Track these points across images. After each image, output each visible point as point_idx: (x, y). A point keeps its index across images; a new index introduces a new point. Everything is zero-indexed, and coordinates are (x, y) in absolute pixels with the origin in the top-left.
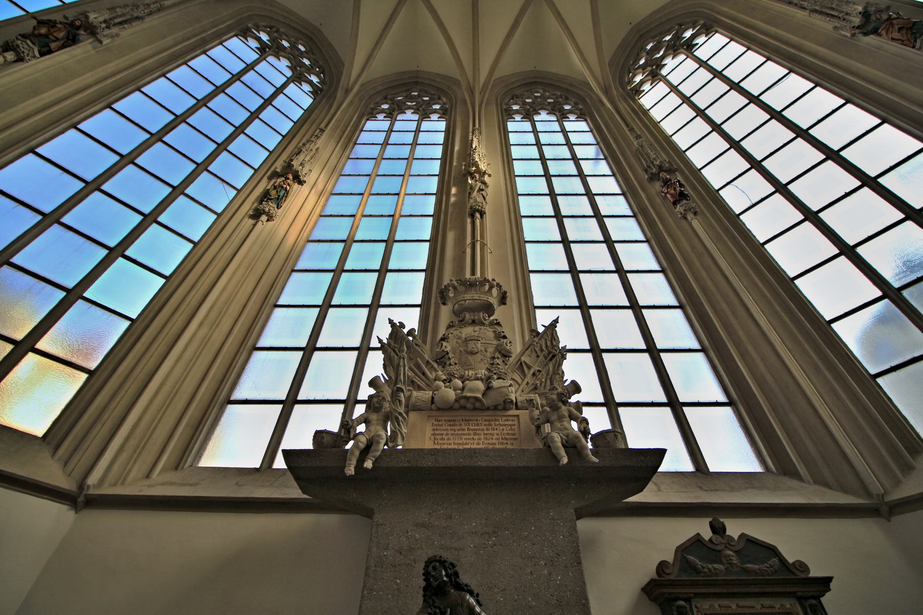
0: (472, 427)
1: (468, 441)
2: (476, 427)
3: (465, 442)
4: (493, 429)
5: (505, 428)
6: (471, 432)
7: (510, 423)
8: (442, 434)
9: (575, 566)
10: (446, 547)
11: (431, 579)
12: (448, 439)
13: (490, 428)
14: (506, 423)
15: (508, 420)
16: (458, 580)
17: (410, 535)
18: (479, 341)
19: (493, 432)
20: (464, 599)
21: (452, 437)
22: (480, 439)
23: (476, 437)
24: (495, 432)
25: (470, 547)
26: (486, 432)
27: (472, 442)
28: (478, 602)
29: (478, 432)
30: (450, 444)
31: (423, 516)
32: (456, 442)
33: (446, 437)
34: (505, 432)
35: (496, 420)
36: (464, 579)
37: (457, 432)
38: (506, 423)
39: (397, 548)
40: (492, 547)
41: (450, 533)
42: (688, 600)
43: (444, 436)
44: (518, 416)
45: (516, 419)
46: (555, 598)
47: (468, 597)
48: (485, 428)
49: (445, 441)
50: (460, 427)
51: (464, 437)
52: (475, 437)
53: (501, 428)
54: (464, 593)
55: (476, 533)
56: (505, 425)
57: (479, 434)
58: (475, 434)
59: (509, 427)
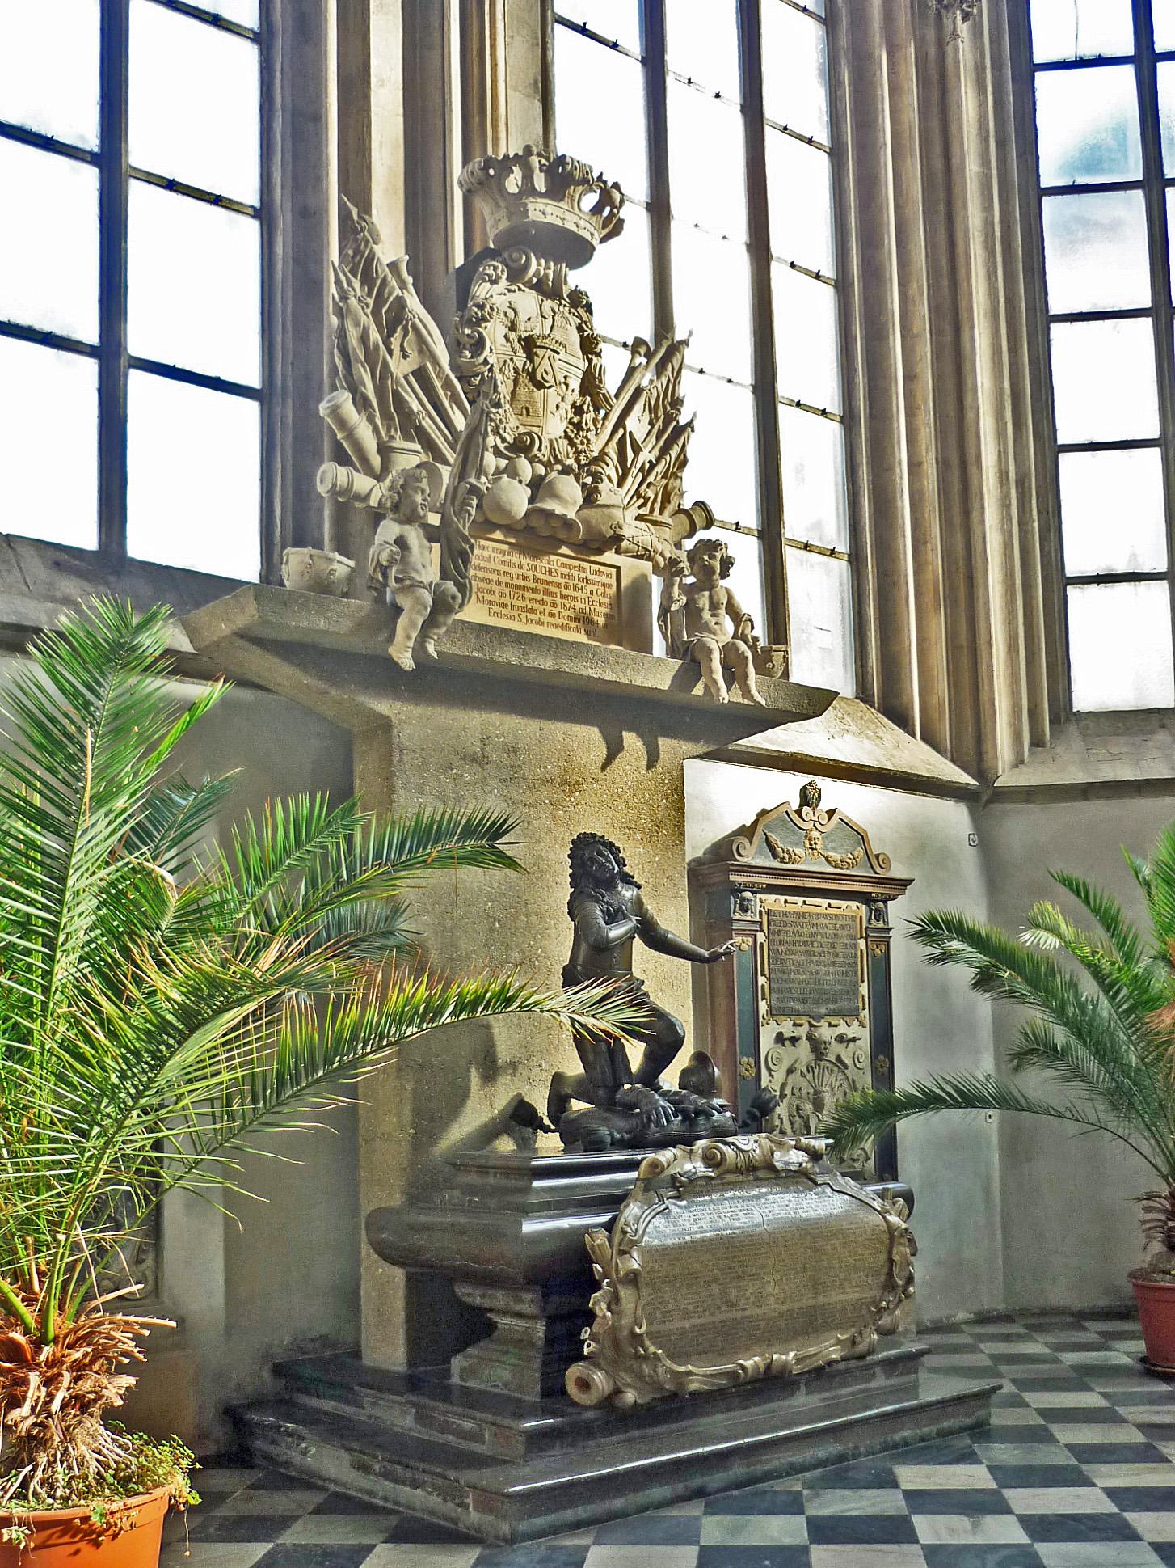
0: (542, 577)
1: (536, 606)
2: (549, 578)
3: (529, 606)
4: (576, 588)
5: (595, 588)
6: (541, 587)
7: (603, 579)
8: (490, 581)
12: (502, 595)
13: (571, 583)
14: (597, 578)
15: (599, 573)
18: (558, 353)
19: (575, 594)
21: (507, 590)
22: (554, 605)
23: (548, 599)
24: (579, 594)
26: (565, 592)
27: (542, 608)
29: (552, 589)
30: (506, 606)
32: (515, 602)
33: (497, 589)
34: (595, 597)
35: (581, 568)
37: (515, 582)
38: (597, 578)
42: (885, 902)
43: (494, 587)
44: (618, 568)
45: (614, 571)
48: (563, 581)
49: (496, 598)
50: (520, 572)
51: (529, 595)
52: (546, 598)
53: (590, 587)
56: (596, 583)
57: (553, 594)
58: (546, 592)
59: (602, 590)
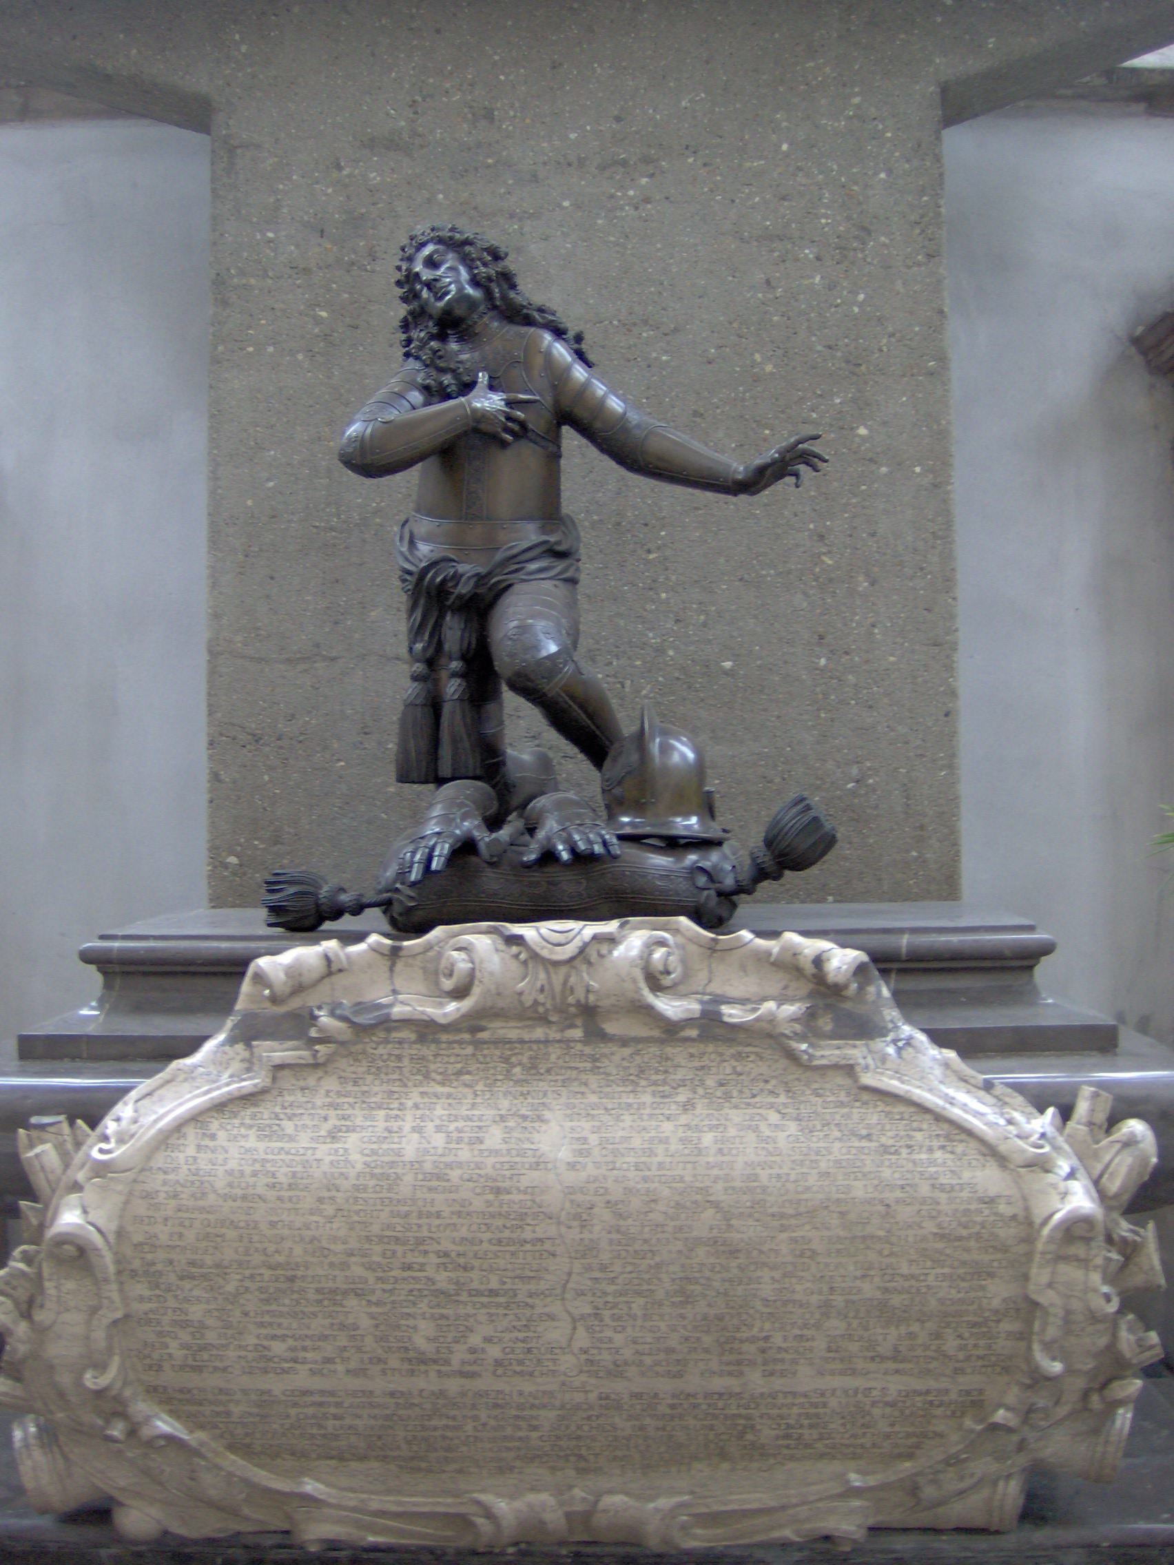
9: (919, 265)
10: (475, 208)
11: (425, 294)
16: (512, 294)
17: (349, 176)
20: (531, 348)
25: (560, 206)
28: (581, 356)
31: (388, 114)
36: (530, 292)
39: (306, 218)
40: (637, 208)
41: (489, 166)
46: (839, 354)
47: (546, 343)
54: (532, 330)
55: (581, 162)
